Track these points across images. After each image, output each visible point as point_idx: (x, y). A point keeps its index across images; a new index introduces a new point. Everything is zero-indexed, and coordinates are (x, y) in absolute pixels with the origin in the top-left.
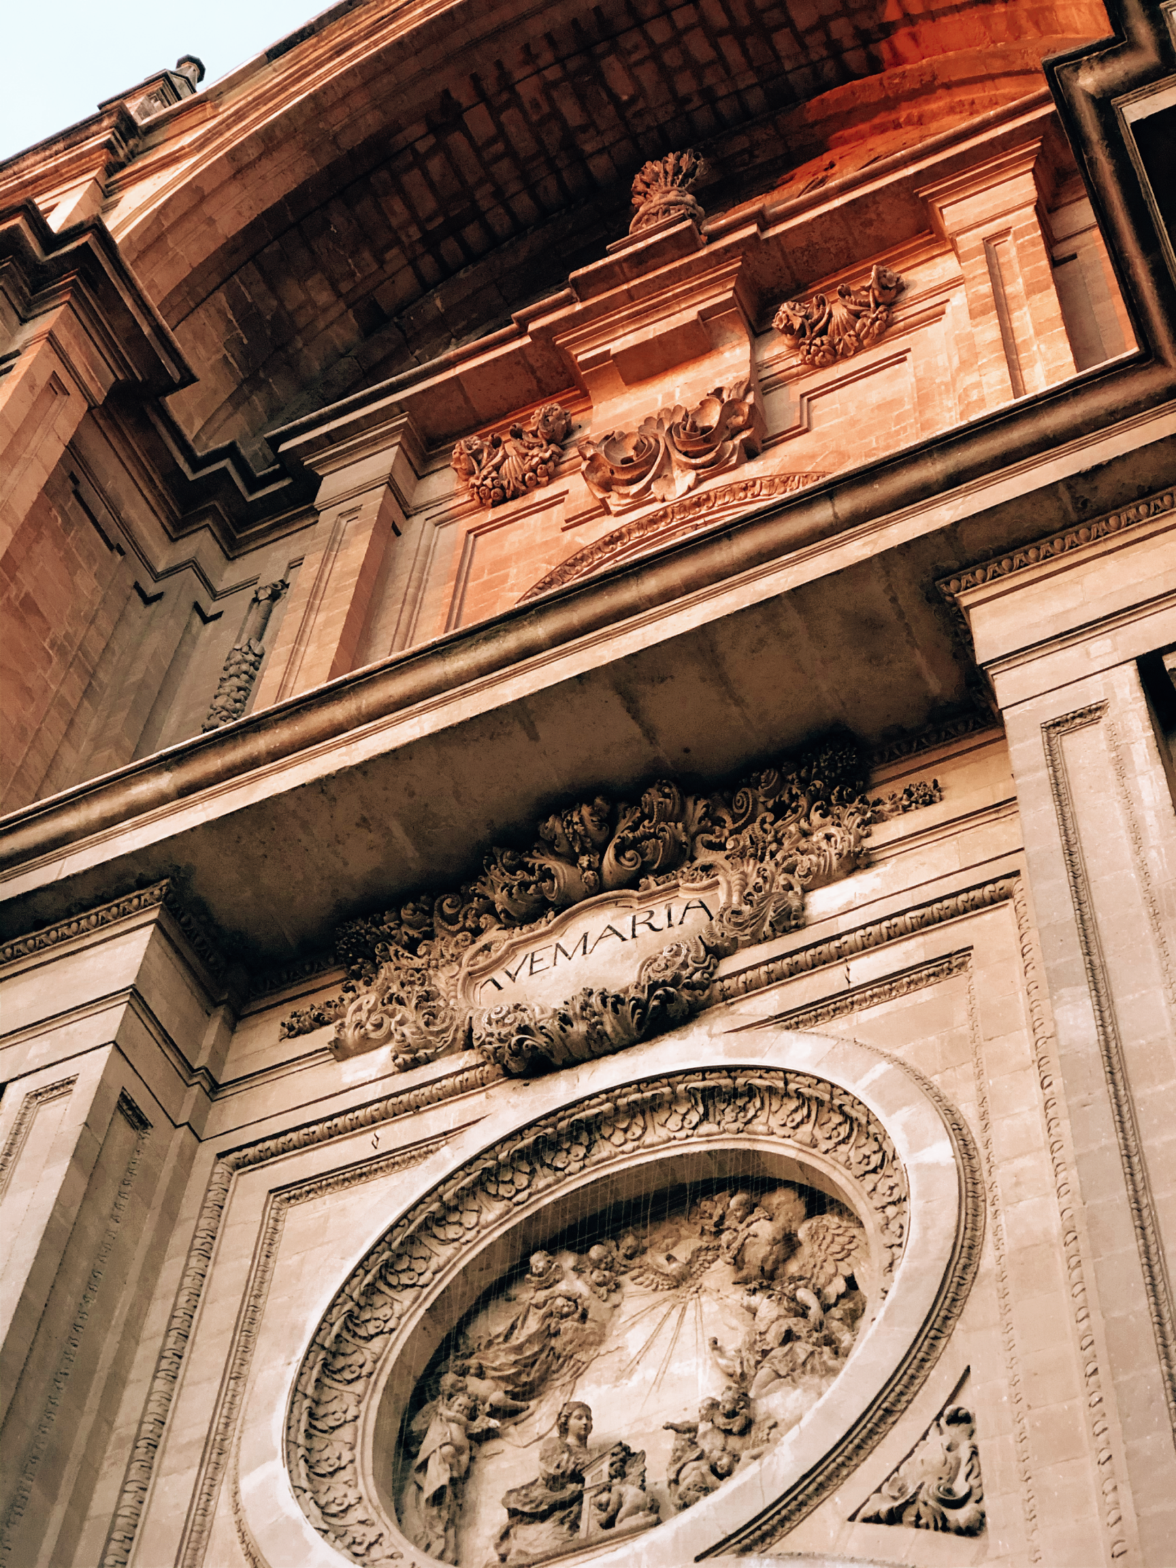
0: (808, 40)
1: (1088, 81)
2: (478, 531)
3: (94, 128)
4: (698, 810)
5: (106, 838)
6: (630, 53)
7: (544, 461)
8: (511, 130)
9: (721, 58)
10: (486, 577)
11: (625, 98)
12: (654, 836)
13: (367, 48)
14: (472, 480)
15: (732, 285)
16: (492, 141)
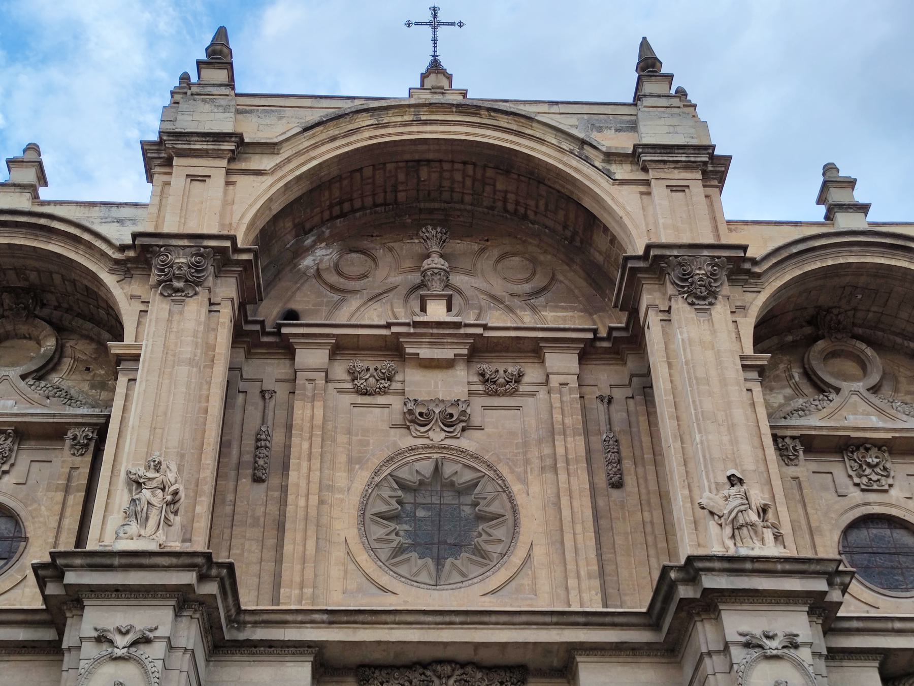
0: (498, 193)
1: (673, 575)
2: (355, 405)
3: (228, 139)
4: (479, 675)
5: (300, 627)
6: (432, 168)
7: (385, 387)
8: (378, 176)
9: (464, 182)
10: (360, 437)
11: (423, 179)
12: (465, 681)
13: (344, 145)
14: (356, 382)
15: (468, 347)
16: (369, 178)
